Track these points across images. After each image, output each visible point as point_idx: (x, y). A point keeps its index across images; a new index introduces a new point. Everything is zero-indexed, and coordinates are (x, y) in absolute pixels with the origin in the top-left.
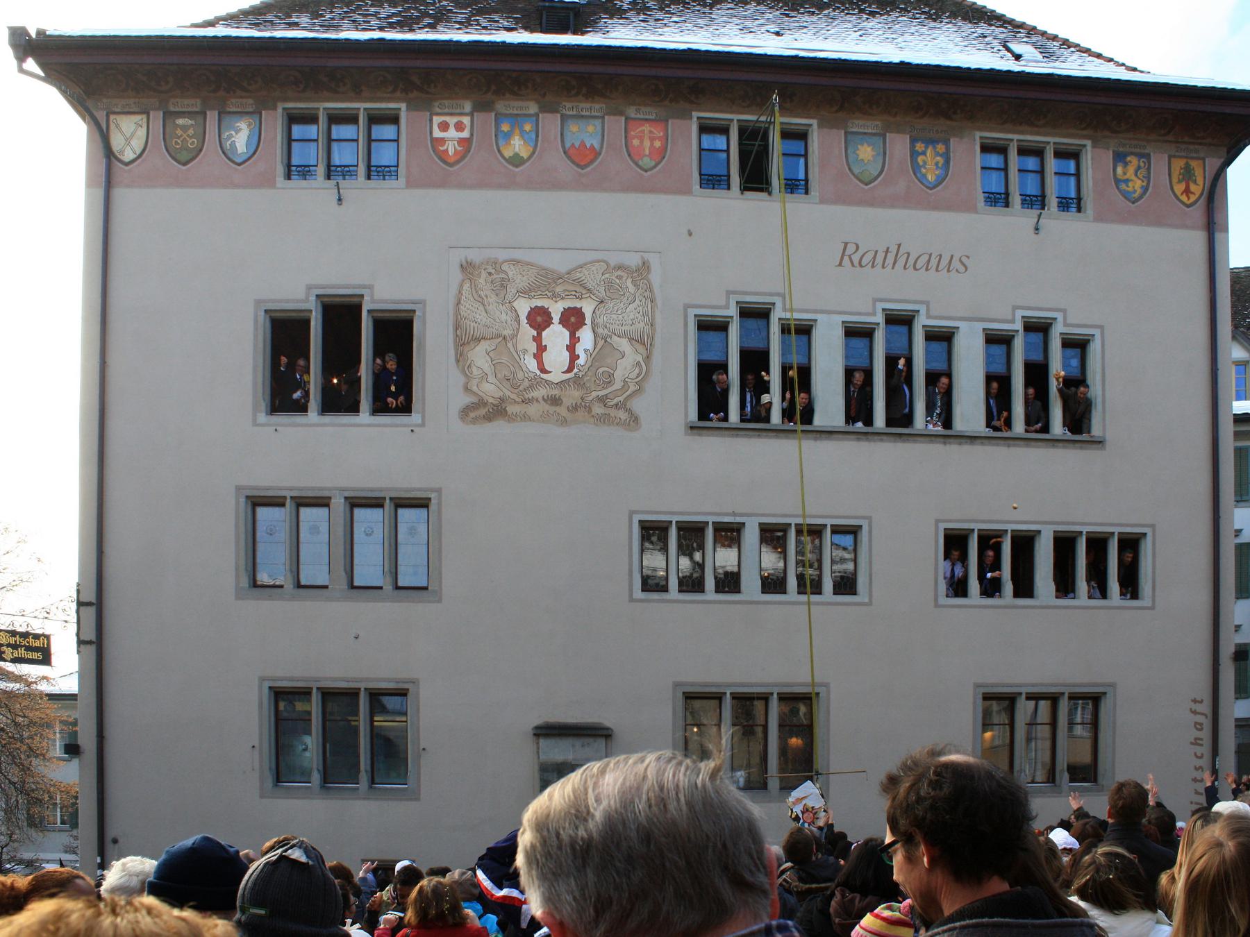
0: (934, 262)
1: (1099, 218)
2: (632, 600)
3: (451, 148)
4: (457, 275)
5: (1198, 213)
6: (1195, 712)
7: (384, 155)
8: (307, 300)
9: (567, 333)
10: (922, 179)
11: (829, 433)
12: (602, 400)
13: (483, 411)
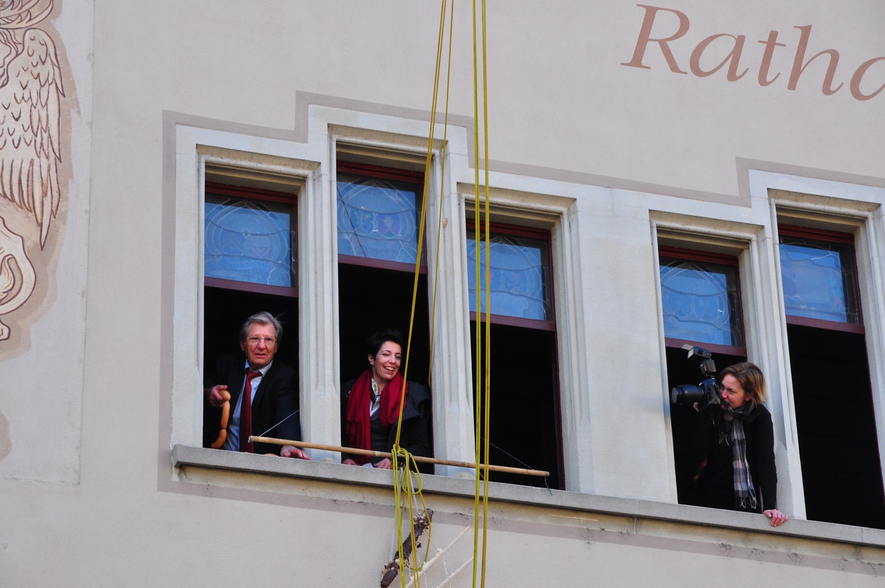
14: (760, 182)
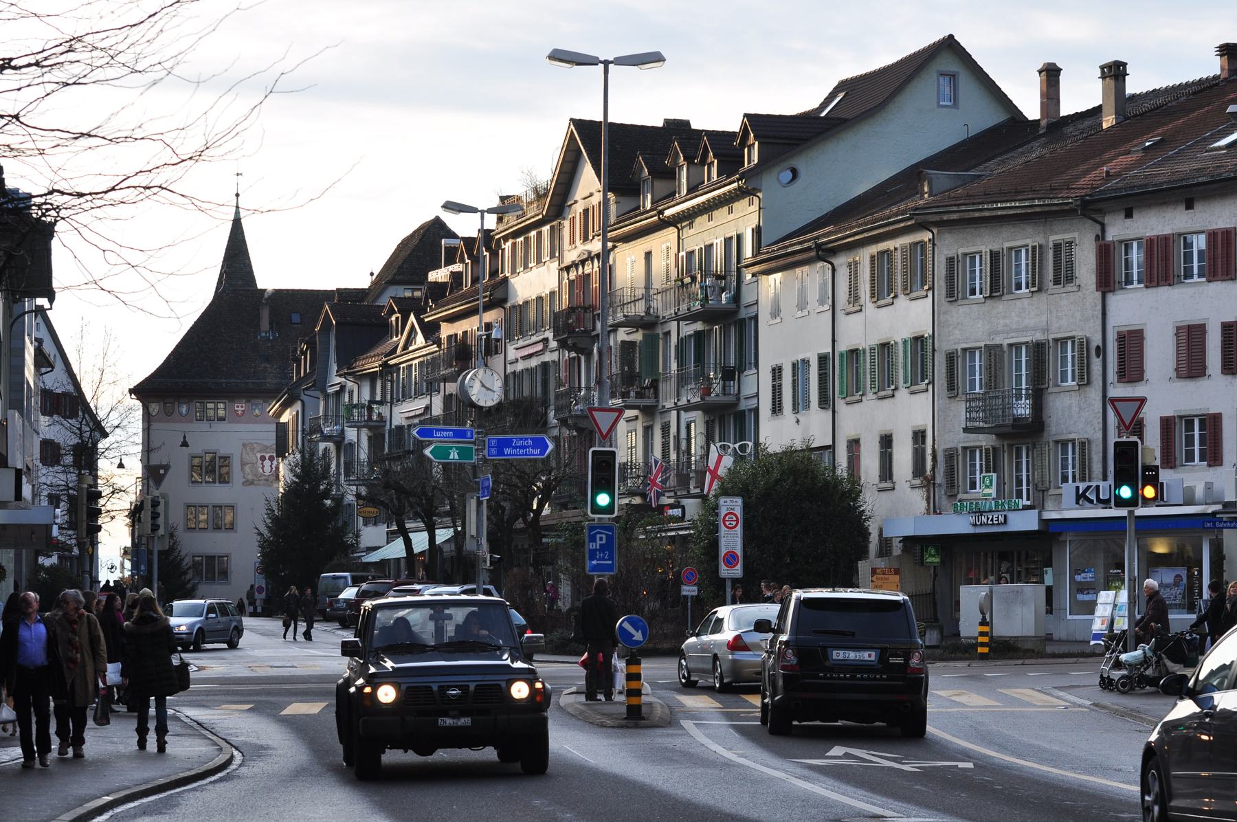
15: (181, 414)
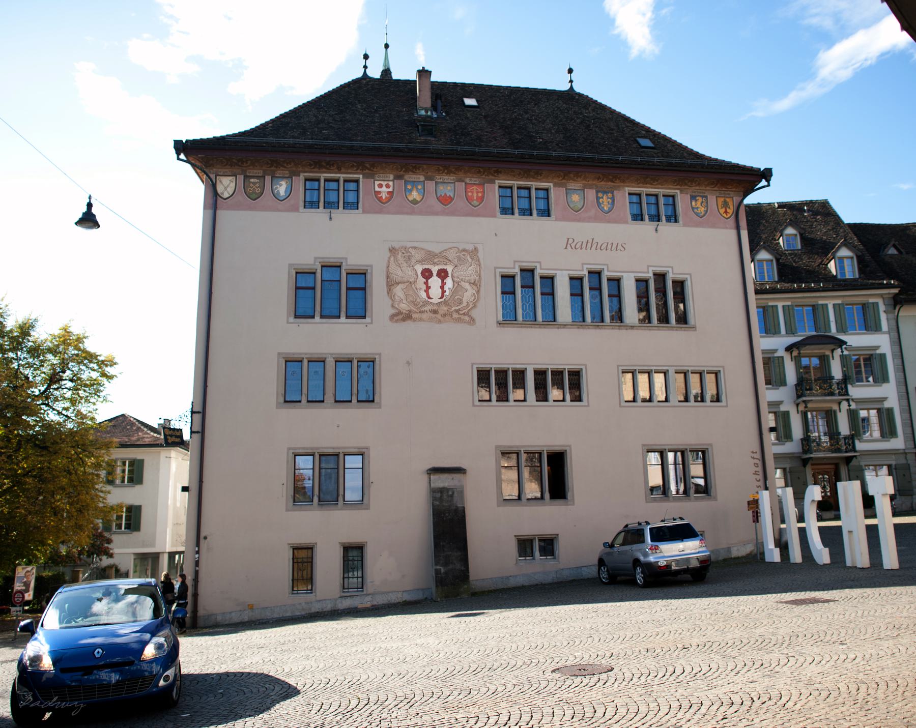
0: (609, 246)
1: (685, 225)
2: (474, 406)
3: (384, 196)
4: (388, 254)
5: (732, 222)
6: (753, 458)
7: (351, 197)
8: (314, 264)
9: (440, 281)
10: (602, 210)
11: (564, 326)
12: (457, 311)
13: (401, 317)
14: (585, 267)
15: (276, 196)
